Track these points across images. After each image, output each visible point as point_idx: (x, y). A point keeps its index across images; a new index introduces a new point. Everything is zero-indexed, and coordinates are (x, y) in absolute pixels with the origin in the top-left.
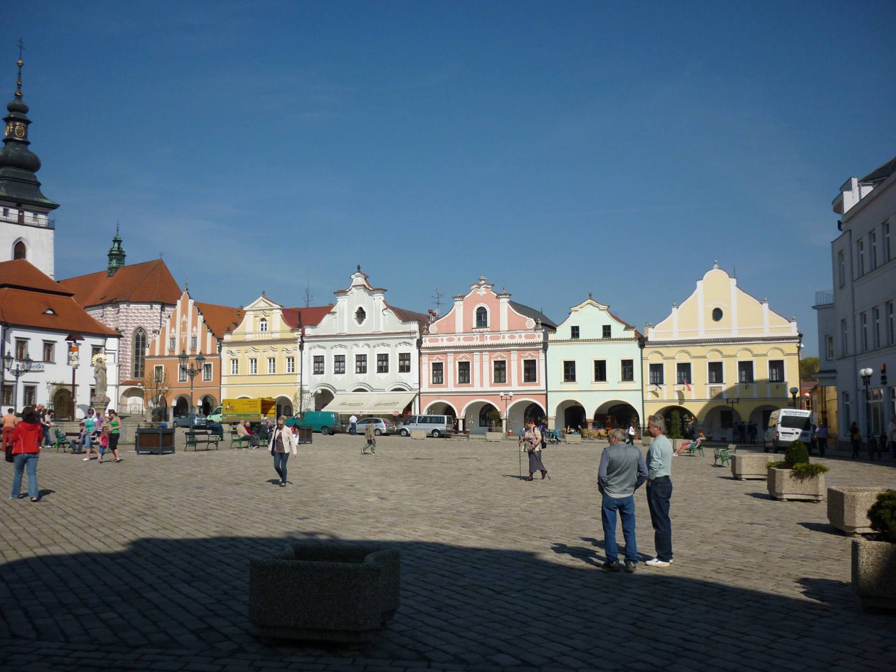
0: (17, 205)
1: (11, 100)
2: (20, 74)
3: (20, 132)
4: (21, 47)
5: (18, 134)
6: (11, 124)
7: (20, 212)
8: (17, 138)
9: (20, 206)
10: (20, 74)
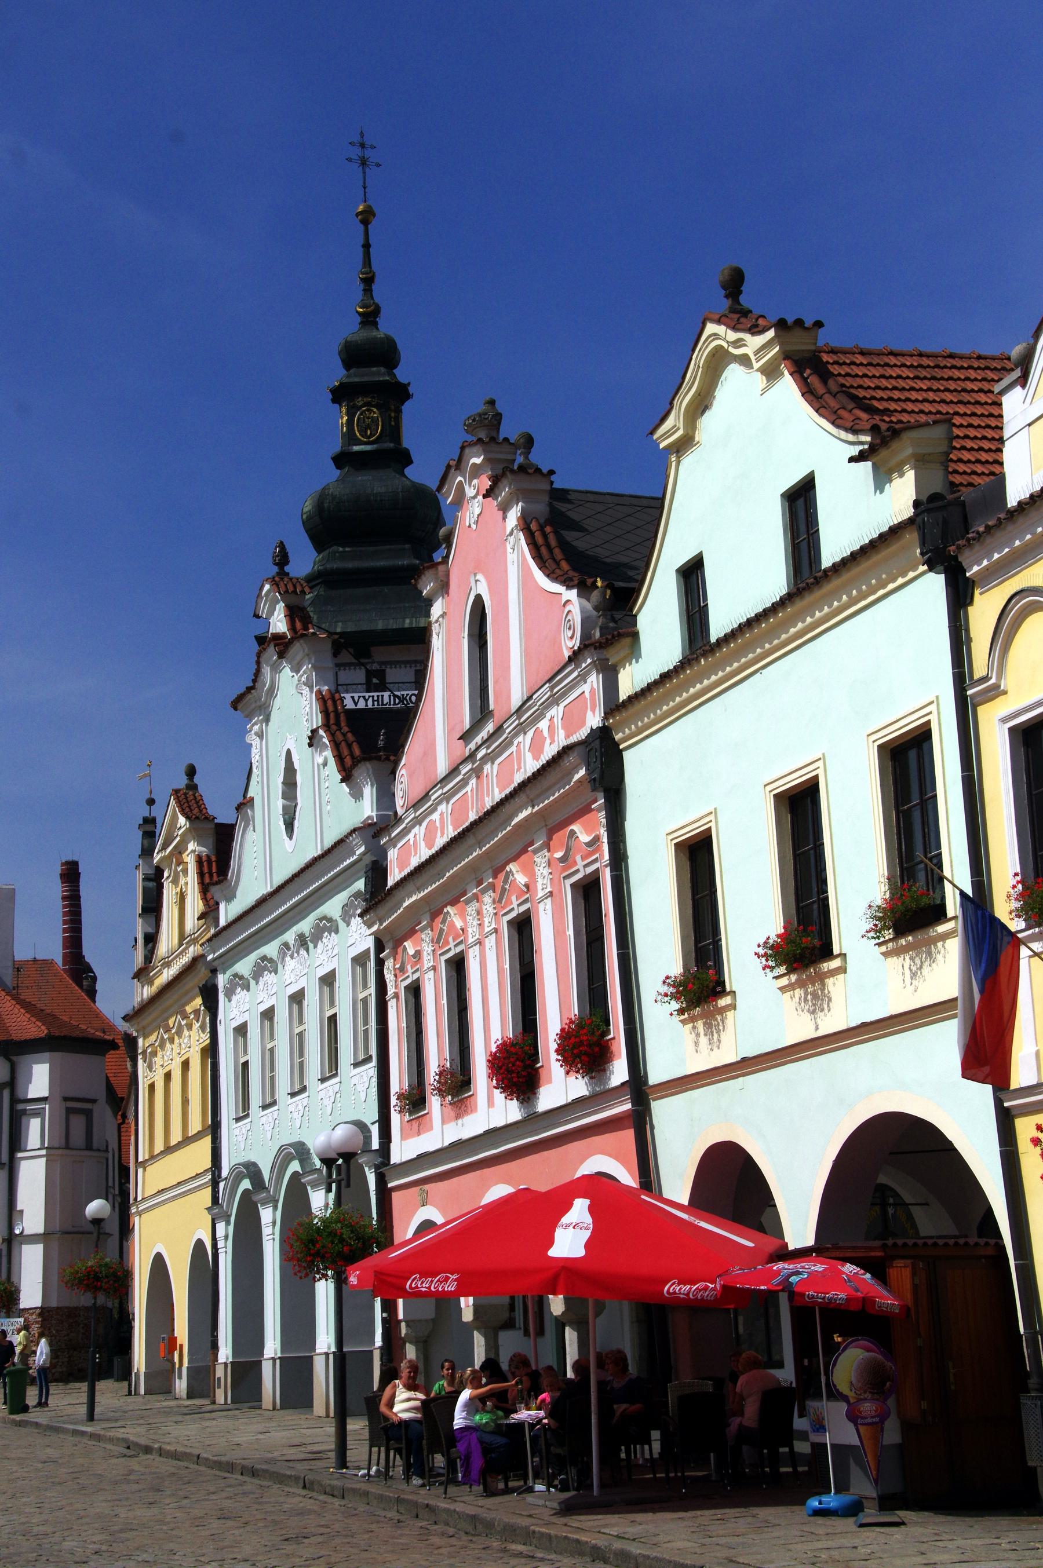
0: (357, 656)
1: (349, 328)
2: (367, 246)
3: (368, 427)
4: (364, 162)
5: (363, 433)
6: (344, 410)
7: (369, 674)
8: (356, 448)
9: (368, 655)
10: (367, 246)
